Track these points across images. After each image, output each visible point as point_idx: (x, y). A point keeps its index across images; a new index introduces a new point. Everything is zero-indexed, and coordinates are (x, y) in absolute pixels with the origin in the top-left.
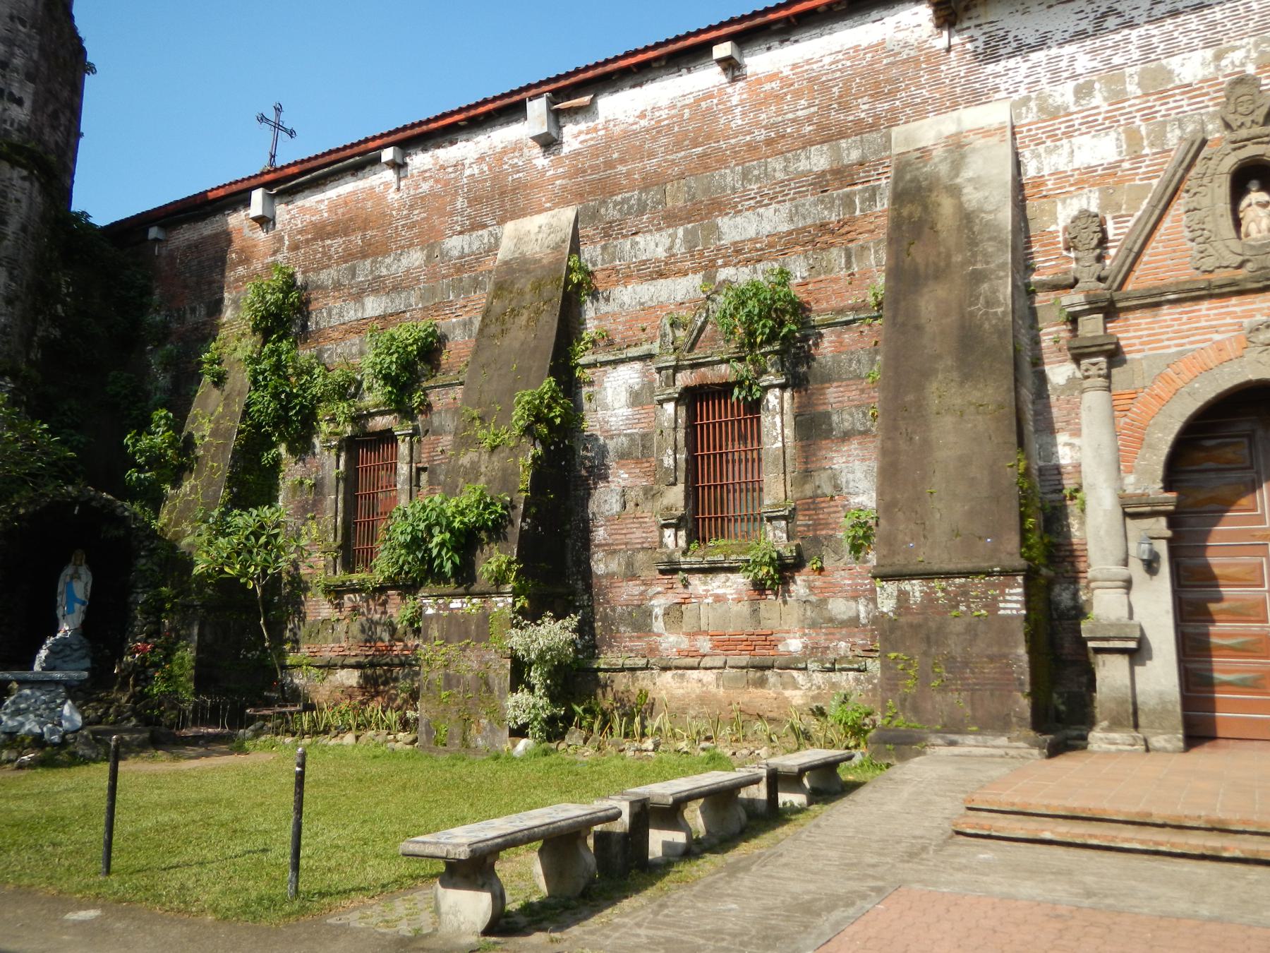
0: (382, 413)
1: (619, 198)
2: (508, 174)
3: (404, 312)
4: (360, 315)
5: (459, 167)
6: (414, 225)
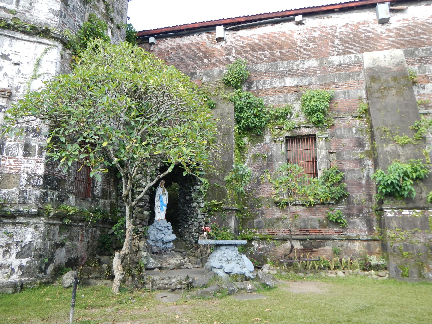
0: (305, 127)
1: (424, 48)
2: (362, 33)
3: (309, 85)
4: (283, 85)
5: (334, 28)
6: (310, 49)
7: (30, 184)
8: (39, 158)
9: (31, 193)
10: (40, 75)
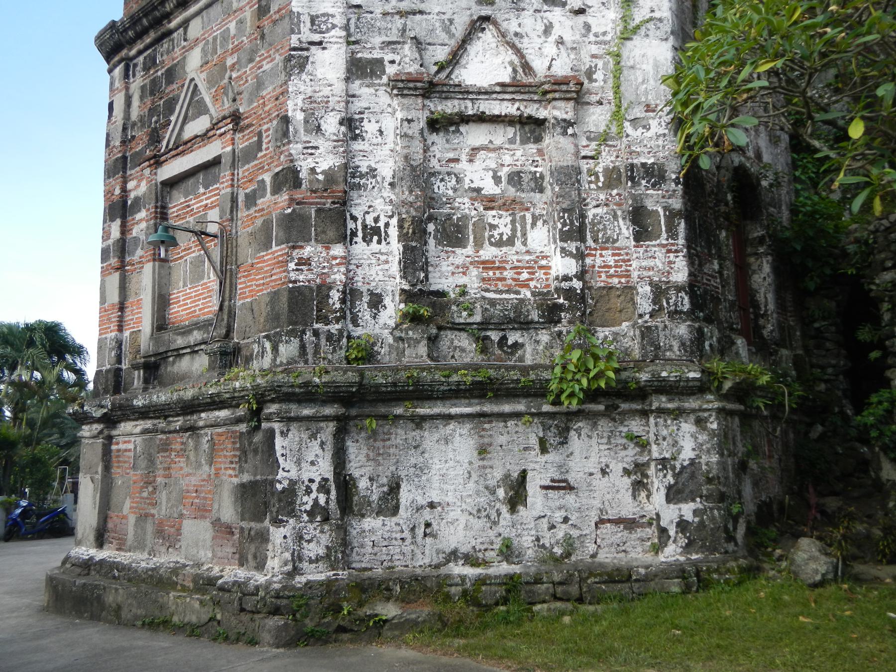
7: (661, 308)
8: (670, 241)
9: (667, 332)
10: (638, 27)
